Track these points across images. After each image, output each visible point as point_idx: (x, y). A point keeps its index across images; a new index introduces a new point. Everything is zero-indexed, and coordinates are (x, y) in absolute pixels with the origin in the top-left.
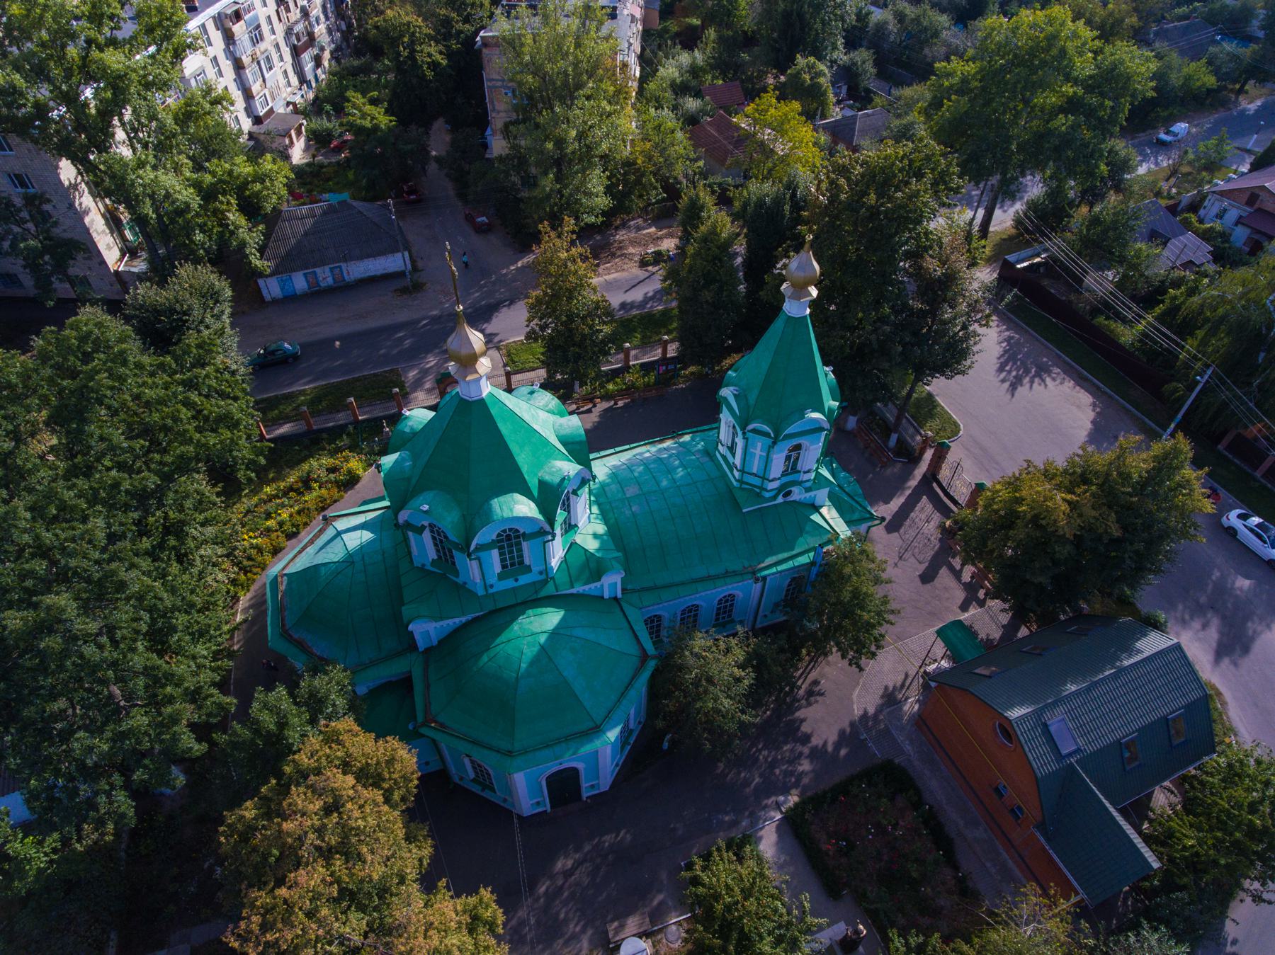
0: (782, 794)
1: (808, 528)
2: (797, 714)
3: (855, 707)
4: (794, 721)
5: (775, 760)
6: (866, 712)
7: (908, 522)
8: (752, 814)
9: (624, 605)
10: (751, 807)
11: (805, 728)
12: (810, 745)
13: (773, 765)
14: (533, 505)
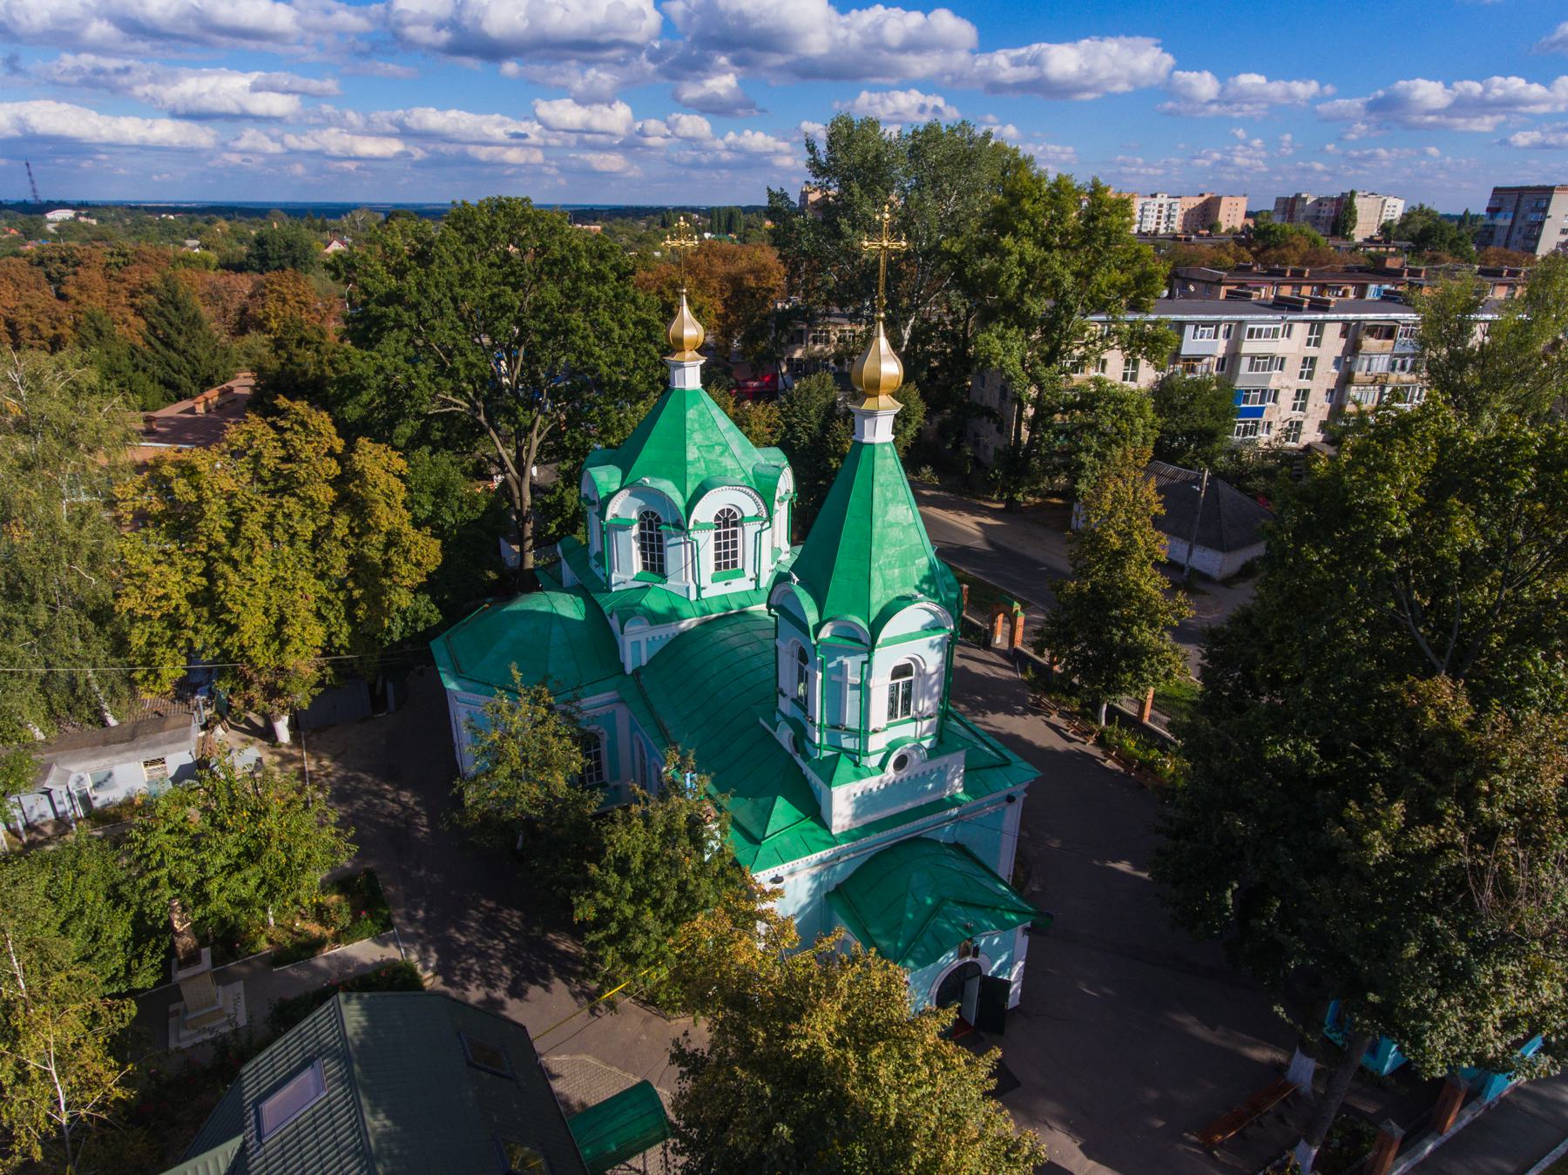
0: (437, 965)
1: (762, 801)
2: (557, 980)
3: (563, 1057)
4: (546, 976)
5: (491, 957)
6: (555, 1077)
9: (618, 678)
10: (433, 936)
11: (535, 991)
12: (507, 999)
13: (482, 955)
14: (616, 486)
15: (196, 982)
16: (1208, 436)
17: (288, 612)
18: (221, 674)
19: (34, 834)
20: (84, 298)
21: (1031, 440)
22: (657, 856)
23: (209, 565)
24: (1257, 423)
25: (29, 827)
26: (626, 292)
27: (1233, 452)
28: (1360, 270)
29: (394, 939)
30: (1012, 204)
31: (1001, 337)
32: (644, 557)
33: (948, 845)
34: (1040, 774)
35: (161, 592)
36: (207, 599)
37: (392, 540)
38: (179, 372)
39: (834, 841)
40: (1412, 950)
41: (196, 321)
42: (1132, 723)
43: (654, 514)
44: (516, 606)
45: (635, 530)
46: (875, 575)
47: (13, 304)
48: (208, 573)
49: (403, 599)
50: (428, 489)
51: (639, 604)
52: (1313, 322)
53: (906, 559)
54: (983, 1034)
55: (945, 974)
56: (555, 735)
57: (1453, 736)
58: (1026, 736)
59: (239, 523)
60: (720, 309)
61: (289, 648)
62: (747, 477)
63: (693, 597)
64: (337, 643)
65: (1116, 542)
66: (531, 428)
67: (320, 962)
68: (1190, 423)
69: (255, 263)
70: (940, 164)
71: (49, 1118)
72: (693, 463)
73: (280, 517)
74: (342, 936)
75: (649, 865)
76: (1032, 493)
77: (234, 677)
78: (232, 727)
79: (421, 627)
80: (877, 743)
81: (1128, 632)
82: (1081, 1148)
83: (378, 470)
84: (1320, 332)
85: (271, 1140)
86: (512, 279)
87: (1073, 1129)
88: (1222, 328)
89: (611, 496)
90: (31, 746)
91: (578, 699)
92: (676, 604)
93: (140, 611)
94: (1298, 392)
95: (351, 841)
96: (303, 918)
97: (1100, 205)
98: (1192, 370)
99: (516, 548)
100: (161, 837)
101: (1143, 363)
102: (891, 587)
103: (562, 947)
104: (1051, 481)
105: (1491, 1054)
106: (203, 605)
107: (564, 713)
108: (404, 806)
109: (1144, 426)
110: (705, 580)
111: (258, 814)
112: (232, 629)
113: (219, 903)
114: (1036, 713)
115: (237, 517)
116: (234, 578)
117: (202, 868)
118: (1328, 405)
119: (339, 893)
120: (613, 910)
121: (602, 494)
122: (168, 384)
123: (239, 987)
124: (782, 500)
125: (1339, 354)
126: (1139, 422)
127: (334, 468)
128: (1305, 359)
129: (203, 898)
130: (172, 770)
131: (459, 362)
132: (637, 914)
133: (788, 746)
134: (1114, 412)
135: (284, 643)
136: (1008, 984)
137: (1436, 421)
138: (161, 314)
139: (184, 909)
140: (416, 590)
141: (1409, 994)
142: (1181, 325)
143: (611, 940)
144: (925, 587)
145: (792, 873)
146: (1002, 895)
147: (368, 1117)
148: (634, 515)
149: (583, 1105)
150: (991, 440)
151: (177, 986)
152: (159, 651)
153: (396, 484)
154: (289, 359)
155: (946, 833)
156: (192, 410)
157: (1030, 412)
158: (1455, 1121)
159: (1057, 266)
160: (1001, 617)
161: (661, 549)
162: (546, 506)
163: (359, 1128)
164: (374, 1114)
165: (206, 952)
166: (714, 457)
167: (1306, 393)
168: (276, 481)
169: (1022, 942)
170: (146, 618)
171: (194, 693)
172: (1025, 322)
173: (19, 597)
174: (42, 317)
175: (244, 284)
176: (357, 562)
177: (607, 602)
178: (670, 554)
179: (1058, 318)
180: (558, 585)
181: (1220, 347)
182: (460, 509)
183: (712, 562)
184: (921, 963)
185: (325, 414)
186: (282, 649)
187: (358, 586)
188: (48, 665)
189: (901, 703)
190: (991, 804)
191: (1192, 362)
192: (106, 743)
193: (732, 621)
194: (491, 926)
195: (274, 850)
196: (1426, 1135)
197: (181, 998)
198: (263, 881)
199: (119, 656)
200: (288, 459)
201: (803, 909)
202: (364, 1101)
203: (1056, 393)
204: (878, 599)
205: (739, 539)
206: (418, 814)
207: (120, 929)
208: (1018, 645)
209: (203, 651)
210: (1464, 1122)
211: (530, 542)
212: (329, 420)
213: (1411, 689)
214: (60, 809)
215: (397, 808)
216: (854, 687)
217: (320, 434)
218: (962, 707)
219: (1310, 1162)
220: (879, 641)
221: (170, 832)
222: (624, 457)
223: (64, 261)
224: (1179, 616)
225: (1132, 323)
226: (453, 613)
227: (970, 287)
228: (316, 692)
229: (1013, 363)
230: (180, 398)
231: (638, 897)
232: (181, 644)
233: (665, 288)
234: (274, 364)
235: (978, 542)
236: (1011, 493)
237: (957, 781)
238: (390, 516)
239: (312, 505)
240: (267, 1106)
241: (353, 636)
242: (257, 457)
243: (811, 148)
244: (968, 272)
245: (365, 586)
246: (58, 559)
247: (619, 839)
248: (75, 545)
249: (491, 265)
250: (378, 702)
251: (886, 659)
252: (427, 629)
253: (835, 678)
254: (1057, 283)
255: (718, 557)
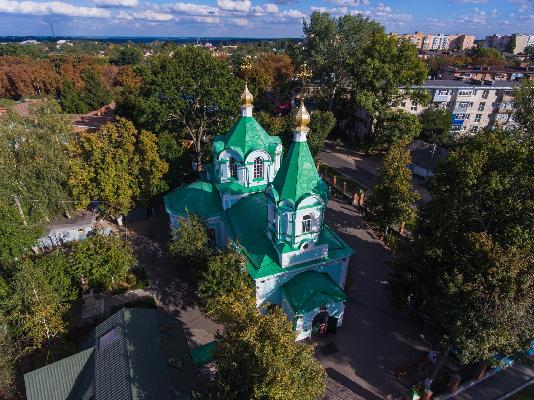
1: (260, 256)
2: (197, 307)
3: (196, 330)
4: (193, 304)
5: (177, 297)
6: (193, 336)
7: (339, 385)
8: (157, 289)
11: (189, 309)
13: (175, 296)
14: (222, 149)
15: (89, 299)
16: (440, 131)
17: (120, 185)
18: (101, 204)
19: (46, 250)
20: (66, 74)
21: (375, 131)
22: (225, 271)
23: (96, 170)
24: (460, 126)
25: (45, 247)
26: (231, 80)
27: (450, 137)
28: (511, 67)
29: (149, 290)
30: (373, 46)
31: (365, 95)
32: (231, 172)
33: (322, 273)
34: (354, 252)
35: (81, 178)
36: (95, 180)
37: (153, 163)
38: (93, 101)
39: (282, 271)
40: (459, 323)
41: (98, 84)
42: (396, 234)
43: (234, 159)
44: (191, 186)
45: (228, 164)
46: (298, 186)
47: (44, 76)
48: (96, 172)
49: (157, 182)
50: (164, 146)
51: (229, 188)
52: (485, 90)
53: (309, 180)
54: (329, 334)
55: (315, 315)
56: (199, 229)
57: (485, 253)
58: (359, 236)
59: (104, 157)
60: (273, 80)
61: (120, 197)
62: (265, 147)
63: (246, 186)
64: (136, 195)
65: (392, 173)
66: (201, 125)
67: (126, 295)
68: (434, 126)
69: (121, 60)
70: (349, 30)
71: (43, 337)
72: (247, 142)
73: (117, 155)
74: (134, 287)
75: (221, 274)
76: (375, 150)
77: (105, 205)
78: (106, 219)
79: (162, 191)
80: (297, 240)
81: (396, 204)
82: (355, 372)
83: (148, 141)
84: (487, 93)
85: (102, 349)
86: (194, 75)
87: (353, 366)
88: (450, 91)
89: (221, 152)
90: (44, 222)
91: (207, 218)
92: (241, 188)
93: (75, 184)
94: (477, 115)
95: (136, 259)
96: (122, 281)
97: (404, 47)
98: (437, 106)
99: (196, 164)
100: (79, 255)
101: (418, 104)
102: (303, 190)
103: (199, 296)
104: (382, 146)
105: (484, 358)
106: (94, 182)
107: (202, 223)
108: (155, 248)
109: (416, 128)
110: (251, 181)
111: (108, 250)
112: (103, 190)
113: (96, 275)
114: (364, 228)
115: (104, 154)
116: (103, 174)
117: (92, 265)
118: (488, 120)
119: (133, 274)
120: (210, 287)
121: (218, 151)
122: (90, 105)
123: (102, 300)
124: (278, 155)
125: (494, 102)
126: (414, 126)
127: (134, 140)
128: (481, 103)
129: (92, 274)
130: (86, 233)
131: (174, 104)
132: (219, 289)
133: (270, 239)
134: (404, 122)
135: (119, 195)
136: (337, 320)
137: (492, 144)
138: (88, 81)
139: (85, 277)
140: (161, 179)
141: (458, 337)
142: (434, 90)
143: (210, 297)
144: (316, 190)
145: (268, 279)
146: (337, 291)
147: (128, 346)
148: (228, 159)
149: (200, 345)
150: (363, 130)
151: (83, 299)
152: (81, 196)
153: (154, 145)
154: (126, 98)
155: (321, 269)
156: (96, 114)
157: (375, 121)
158: (483, 376)
159: (387, 70)
160: (356, 194)
161: (236, 170)
162: (205, 151)
163: (125, 349)
164: (130, 344)
165: (92, 290)
166: (255, 140)
167: (480, 115)
168: (116, 143)
169: (343, 307)
170: (77, 186)
171: (94, 208)
172: (375, 90)
173: (40, 178)
174: (53, 80)
175: (116, 69)
176: (142, 170)
177: (219, 187)
178: (239, 172)
179: (387, 88)
180: (206, 180)
181: (449, 98)
182: (175, 153)
183: (253, 175)
184: (307, 311)
185: (131, 122)
186: (118, 197)
187: (142, 177)
188: (49, 199)
189: (306, 227)
190: (337, 261)
191: (437, 104)
192: (67, 223)
193: (259, 195)
194: (178, 287)
195: (113, 261)
196: (472, 380)
197: (84, 303)
198: (110, 269)
199: (70, 197)
200: (120, 136)
201: (272, 290)
202: (127, 341)
203: (385, 115)
204: (299, 194)
205: (262, 168)
206: (159, 251)
207: (67, 282)
208: (361, 205)
209: (94, 196)
210: (487, 377)
211: (200, 163)
212: (132, 124)
213: (472, 236)
214: (53, 242)
215: (153, 248)
216: (290, 222)
217: (129, 128)
218: (339, 225)
219: (430, 384)
220: (298, 208)
221: (82, 253)
222: (226, 137)
223: (60, 60)
224: (415, 199)
225: (415, 89)
226: (173, 187)
227: (357, 76)
228: (130, 210)
229: (369, 104)
230: (94, 109)
231: (218, 284)
232: (88, 194)
233: (253, 72)
234: (121, 100)
235: (354, 167)
236: (367, 149)
237: (325, 253)
238: (151, 155)
239: (128, 151)
240: (101, 339)
241: (140, 193)
242: (110, 136)
243: (305, 24)
244: (355, 71)
245: (144, 178)
246: (50, 167)
247: (212, 266)
248: (55, 163)
249: (187, 70)
250: (149, 214)
251: (300, 214)
252: (164, 192)
253: (284, 218)
254: (387, 76)
255: (255, 173)
